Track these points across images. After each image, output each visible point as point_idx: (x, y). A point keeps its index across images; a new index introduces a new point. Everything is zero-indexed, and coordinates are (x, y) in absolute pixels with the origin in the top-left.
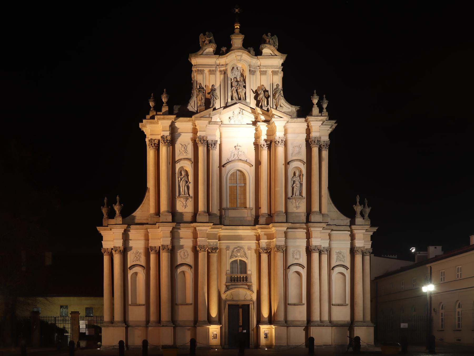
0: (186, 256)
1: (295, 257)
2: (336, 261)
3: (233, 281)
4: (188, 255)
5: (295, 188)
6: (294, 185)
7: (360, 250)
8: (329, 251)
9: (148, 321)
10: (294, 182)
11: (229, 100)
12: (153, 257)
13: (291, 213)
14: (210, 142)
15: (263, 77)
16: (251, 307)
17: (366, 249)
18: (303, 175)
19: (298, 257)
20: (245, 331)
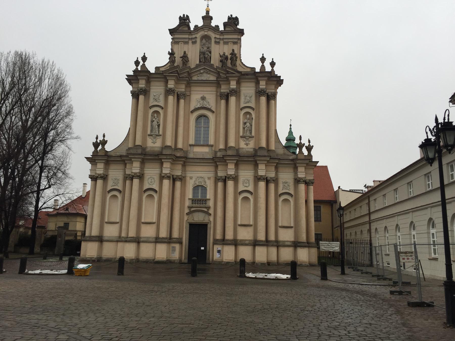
0: (153, 182)
1: (245, 184)
2: (283, 189)
3: (194, 204)
4: (154, 181)
5: (245, 129)
6: (246, 126)
7: (302, 181)
8: (276, 181)
9: (120, 237)
10: (245, 123)
11: (198, 62)
12: (128, 182)
13: (242, 148)
14: (179, 93)
15: (226, 46)
16: (209, 226)
17: (309, 180)
18: (252, 118)
19: (247, 185)
20: (202, 248)
